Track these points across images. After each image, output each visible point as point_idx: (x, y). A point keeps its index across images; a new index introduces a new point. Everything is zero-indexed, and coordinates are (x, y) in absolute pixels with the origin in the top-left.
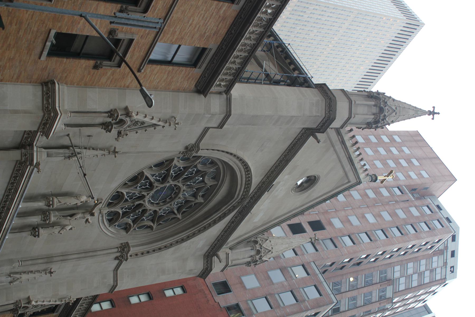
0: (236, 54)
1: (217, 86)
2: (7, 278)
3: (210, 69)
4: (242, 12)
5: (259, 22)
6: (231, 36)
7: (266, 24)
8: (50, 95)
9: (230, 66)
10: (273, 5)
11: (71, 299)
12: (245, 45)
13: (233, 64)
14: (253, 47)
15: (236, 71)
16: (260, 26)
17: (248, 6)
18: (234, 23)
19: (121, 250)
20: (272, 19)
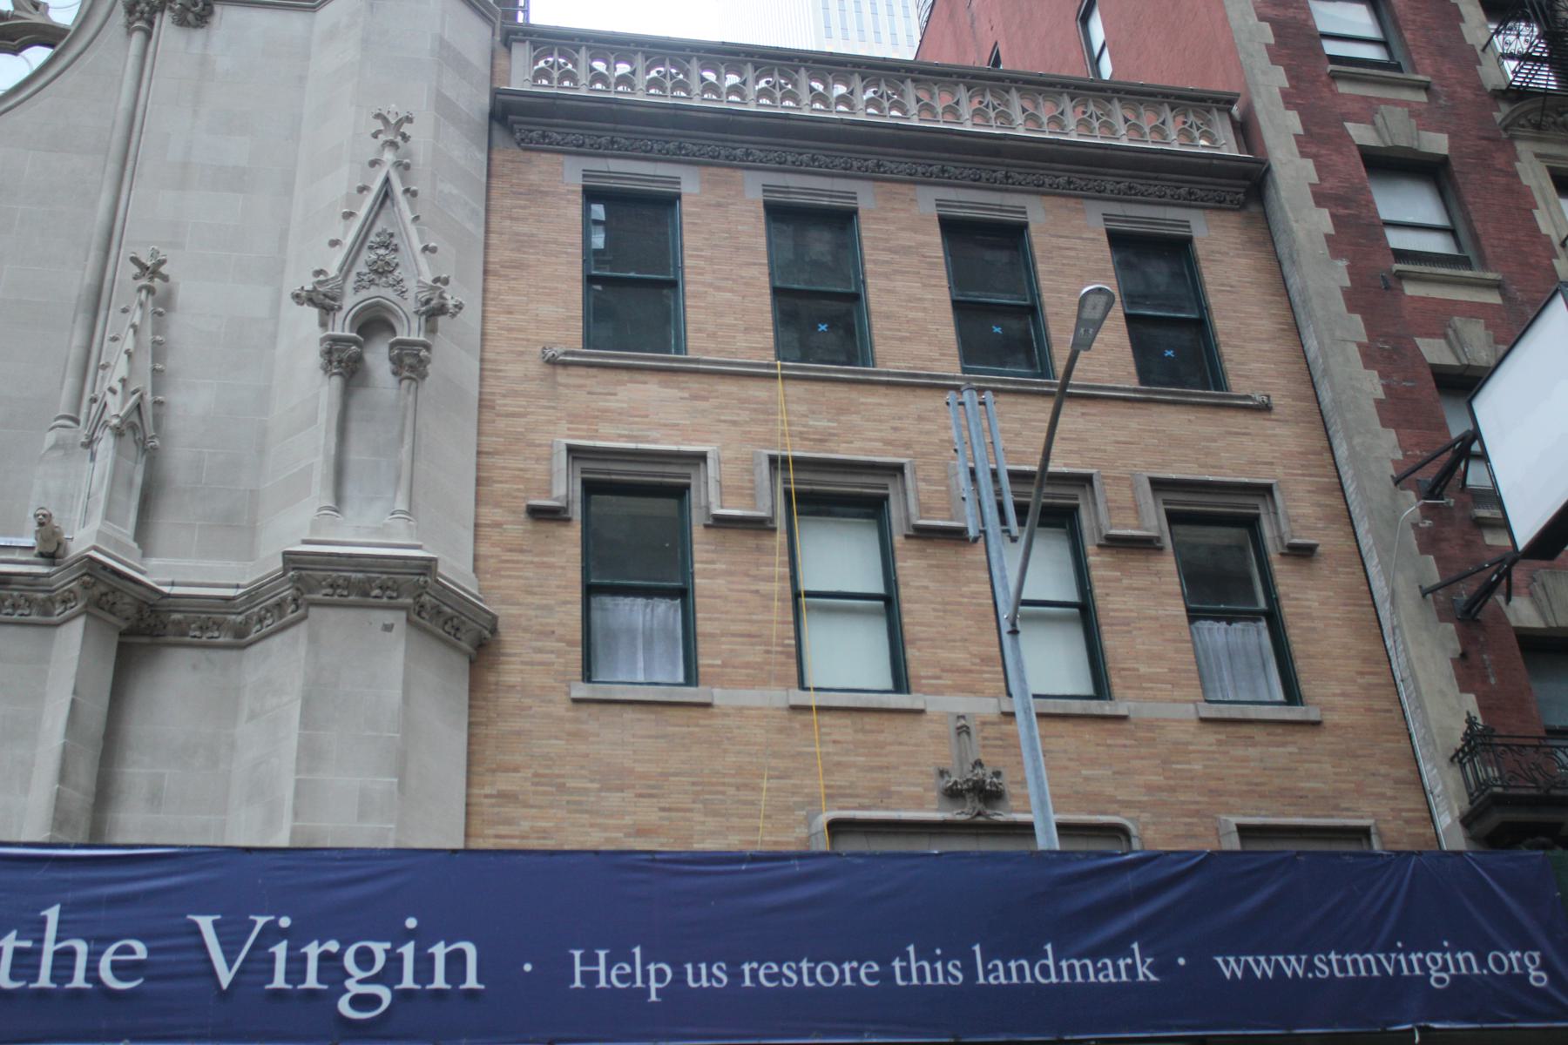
0: (1176, 143)
1: (935, 117)
2: (98, 457)
3: (1034, 178)
4: (727, 157)
5: (1096, 124)
6: (953, 169)
7: (886, 81)
8: (21, 596)
9: (1175, 137)
10: (812, 90)
11: (382, 128)
12: (1185, 133)
13: (1164, 130)
14: (873, 74)
15: (1187, 110)
16: (1208, 126)
17: (1086, 185)
18: (1097, 194)
19: (138, 19)
20: (1172, 100)
